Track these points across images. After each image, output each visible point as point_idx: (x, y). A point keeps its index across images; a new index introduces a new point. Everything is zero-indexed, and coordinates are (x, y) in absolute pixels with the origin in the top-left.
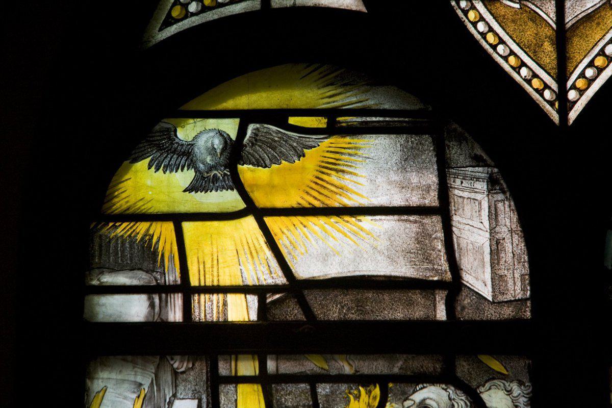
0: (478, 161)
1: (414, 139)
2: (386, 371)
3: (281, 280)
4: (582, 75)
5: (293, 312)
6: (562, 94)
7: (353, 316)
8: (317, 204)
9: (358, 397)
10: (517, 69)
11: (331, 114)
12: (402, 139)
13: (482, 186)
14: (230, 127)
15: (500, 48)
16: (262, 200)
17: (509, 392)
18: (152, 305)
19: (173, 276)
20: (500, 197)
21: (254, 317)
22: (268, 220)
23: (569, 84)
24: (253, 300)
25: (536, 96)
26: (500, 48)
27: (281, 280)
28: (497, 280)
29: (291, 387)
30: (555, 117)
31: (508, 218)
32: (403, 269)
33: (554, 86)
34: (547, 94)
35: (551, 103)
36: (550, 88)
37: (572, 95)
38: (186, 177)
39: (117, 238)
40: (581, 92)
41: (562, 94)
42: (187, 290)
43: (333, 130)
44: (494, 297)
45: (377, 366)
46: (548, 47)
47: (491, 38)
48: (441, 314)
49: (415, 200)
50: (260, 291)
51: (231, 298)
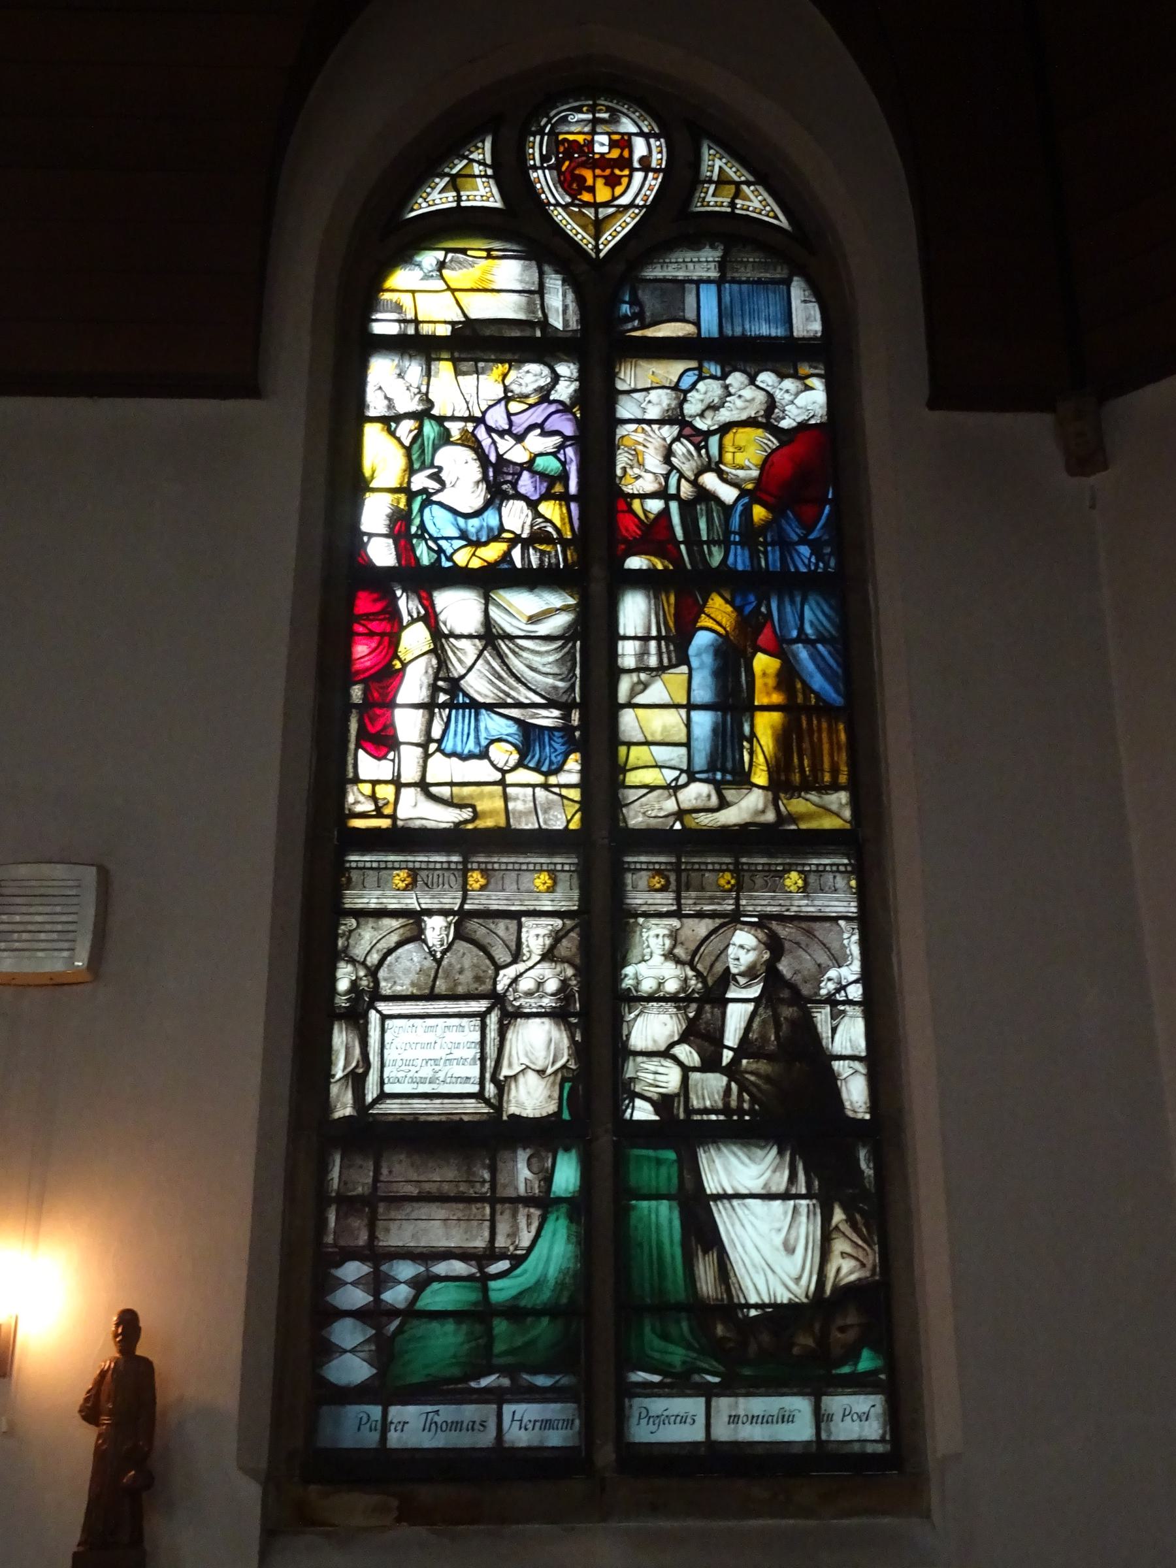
0: (557, 272)
1: (527, 262)
2: (511, 358)
3: (463, 319)
4: (606, 239)
5: (468, 332)
6: (596, 247)
7: (496, 334)
8: (481, 288)
9: (497, 368)
10: (576, 235)
11: (488, 251)
12: (522, 262)
13: (560, 282)
14: (440, 255)
15: (569, 227)
16: (453, 286)
17: (569, 367)
18: (400, 328)
19: (410, 315)
20: (567, 287)
21: (449, 333)
22: (457, 294)
23: (600, 242)
24: (449, 327)
25: (585, 247)
26: (569, 227)
27: (463, 319)
28: (566, 323)
29: (466, 363)
30: (594, 255)
31: (570, 296)
32: (521, 316)
33: (593, 243)
34: (590, 246)
35: (592, 250)
36: (590, 243)
37: (601, 247)
38: (421, 274)
39: (384, 300)
40: (605, 245)
41: (596, 247)
42: (416, 322)
43: (489, 257)
44: (564, 327)
45: (509, 356)
46: (591, 228)
47: (564, 222)
48: (538, 334)
49: (527, 287)
50: (453, 323)
51: (437, 325)
